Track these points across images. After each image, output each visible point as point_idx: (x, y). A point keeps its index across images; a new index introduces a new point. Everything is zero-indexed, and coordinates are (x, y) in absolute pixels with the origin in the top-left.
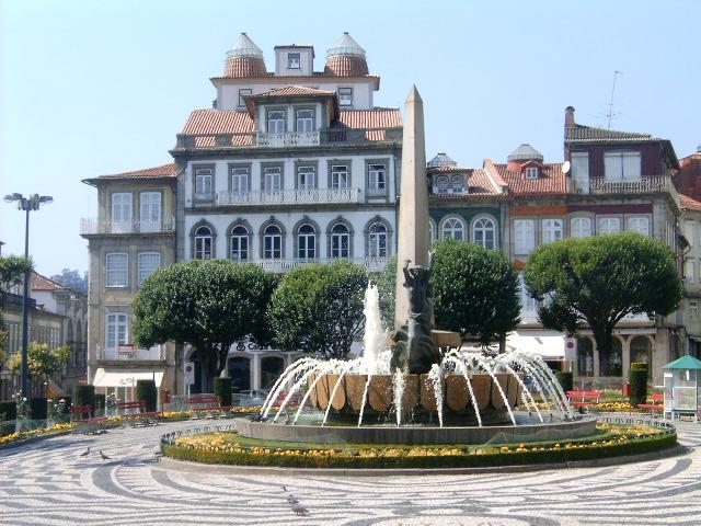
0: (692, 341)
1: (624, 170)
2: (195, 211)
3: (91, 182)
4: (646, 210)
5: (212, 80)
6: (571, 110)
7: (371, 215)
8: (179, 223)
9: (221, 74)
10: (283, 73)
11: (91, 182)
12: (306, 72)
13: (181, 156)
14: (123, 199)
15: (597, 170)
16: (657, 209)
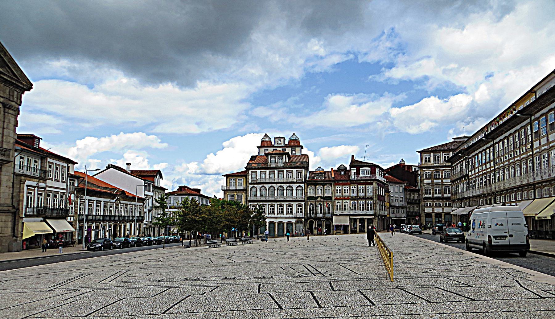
0: (392, 220)
1: (364, 173)
2: (251, 184)
3: (224, 176)
4: (372, 184)
5: (258, 147)
6: (353, 156)
7: (298, 185)
8: (247, 187)
9: (260, 145)
10: (276, 145)
11: (224, 176)
12: (283, 145)
13: (248, 169)
14: (232, 180)
15: (358, 173)
16: (374, 183)
